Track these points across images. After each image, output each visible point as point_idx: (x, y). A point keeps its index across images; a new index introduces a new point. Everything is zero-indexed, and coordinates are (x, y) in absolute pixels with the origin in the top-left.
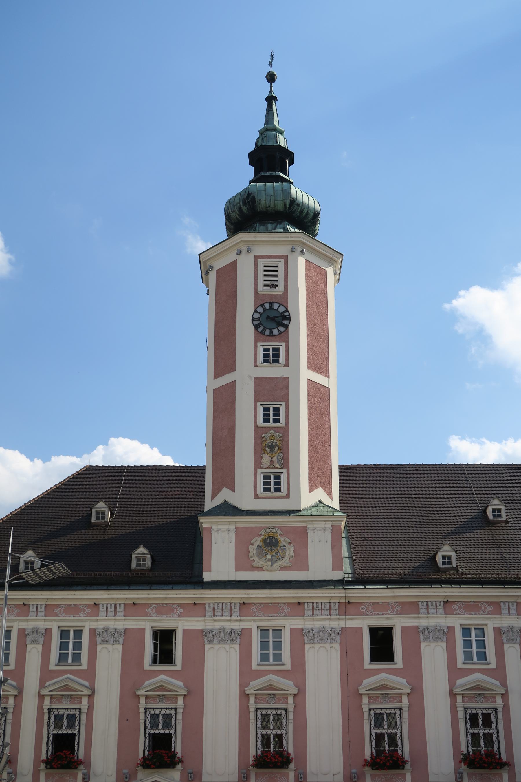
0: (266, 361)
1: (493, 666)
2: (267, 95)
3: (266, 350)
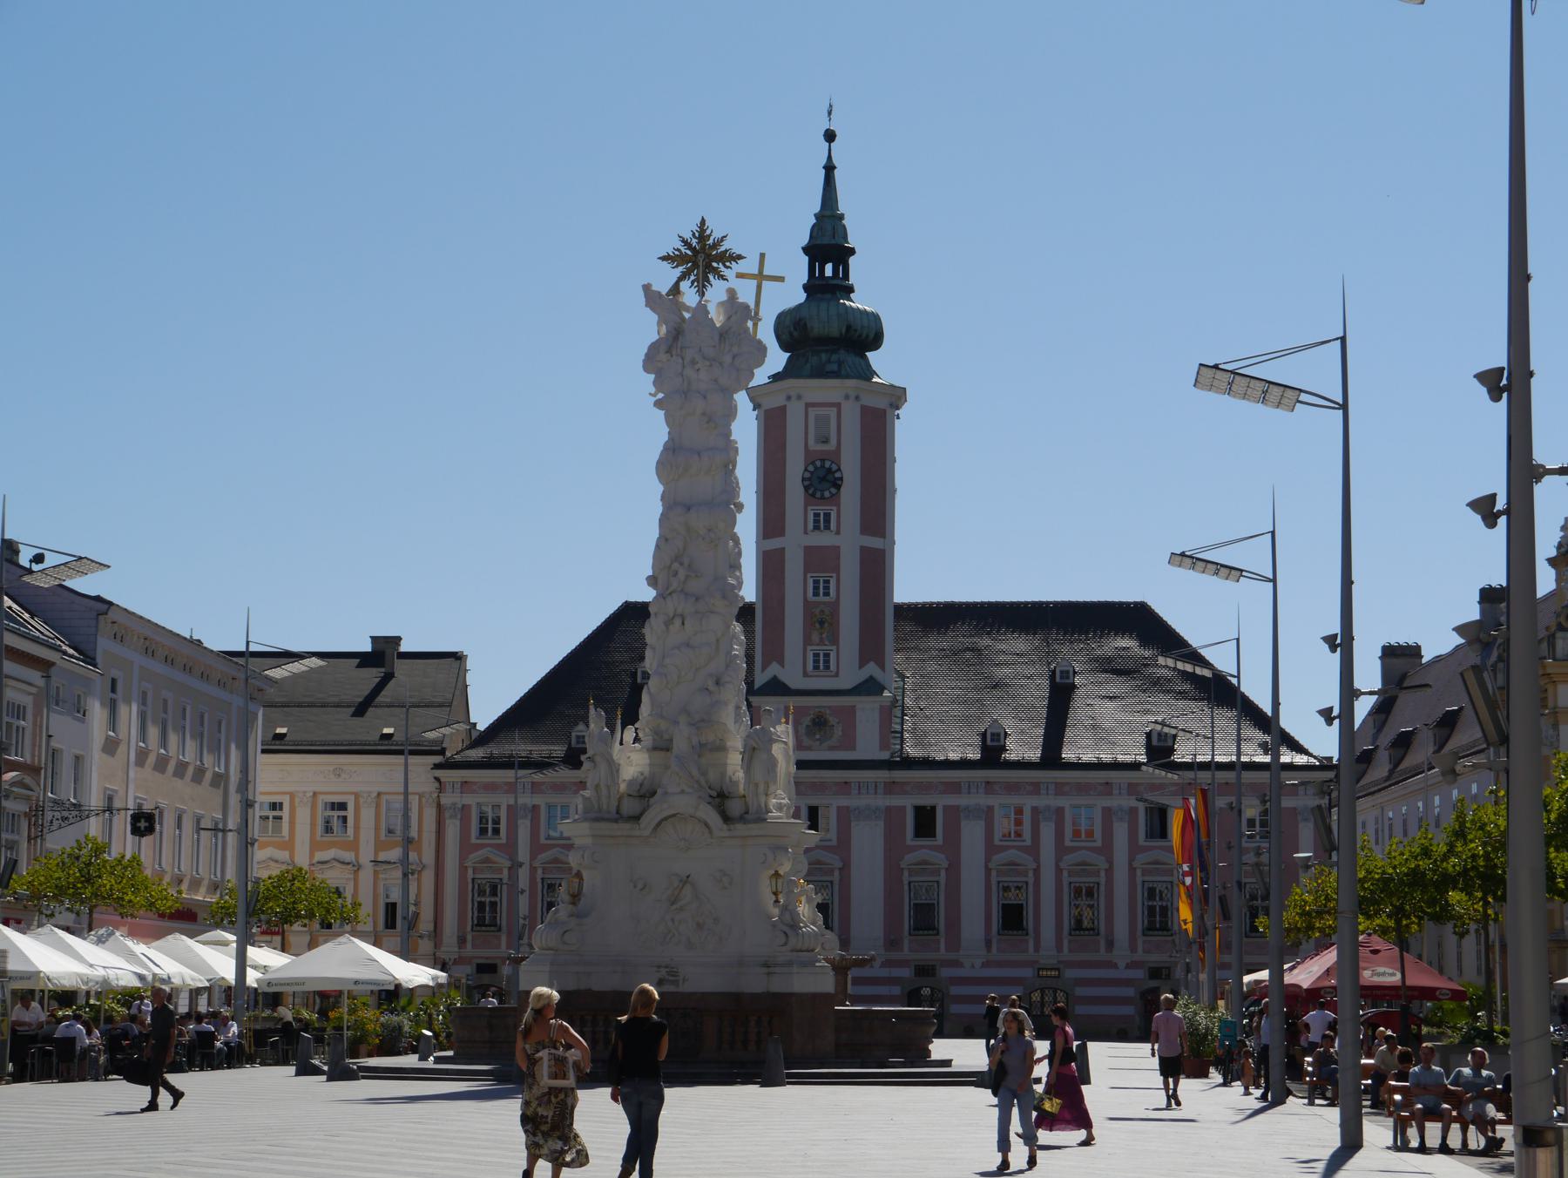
0: (816, 528)
2: (824, 161)
3: (817, 515)
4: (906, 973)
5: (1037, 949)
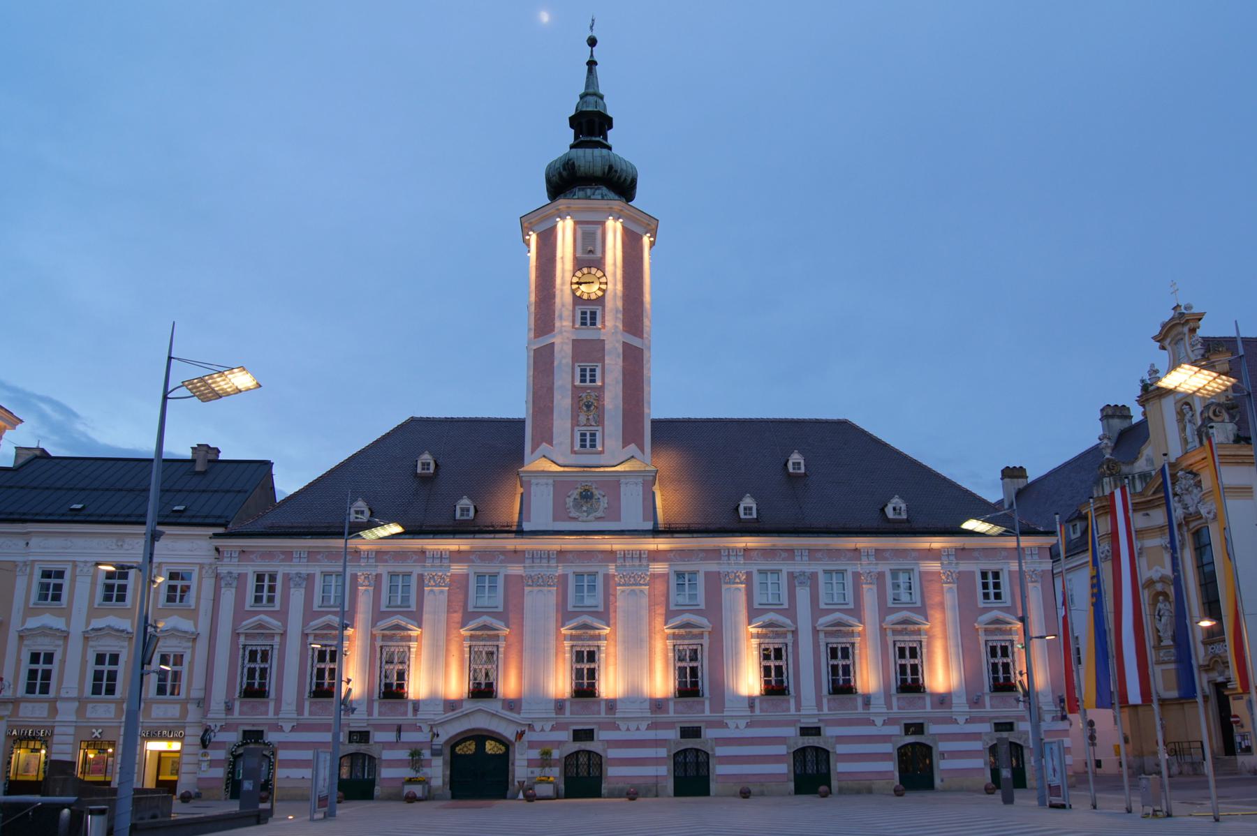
0: (583, 324)
1: (786, 606)
3: (584, 313)
4: (673, 734)
5: (798, 708)
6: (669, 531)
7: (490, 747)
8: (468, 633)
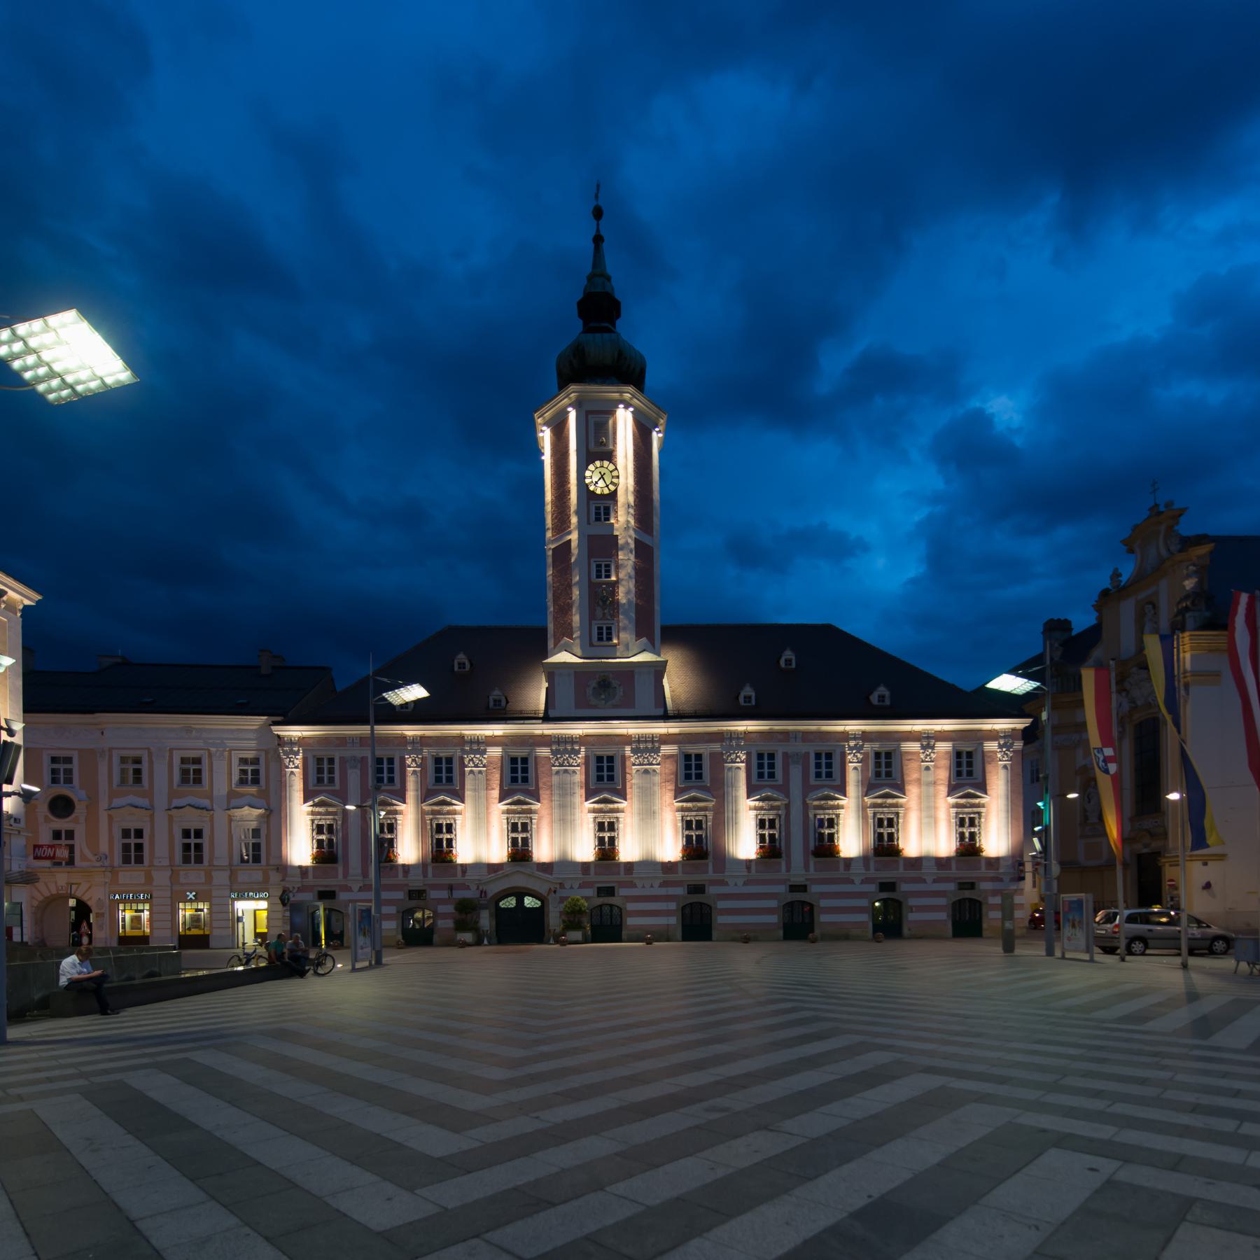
1: (780, 782)
4: (680, 891)
5: (788, 870)
6: (679, 716)
7: (529, 902)
8: (506, 807)
